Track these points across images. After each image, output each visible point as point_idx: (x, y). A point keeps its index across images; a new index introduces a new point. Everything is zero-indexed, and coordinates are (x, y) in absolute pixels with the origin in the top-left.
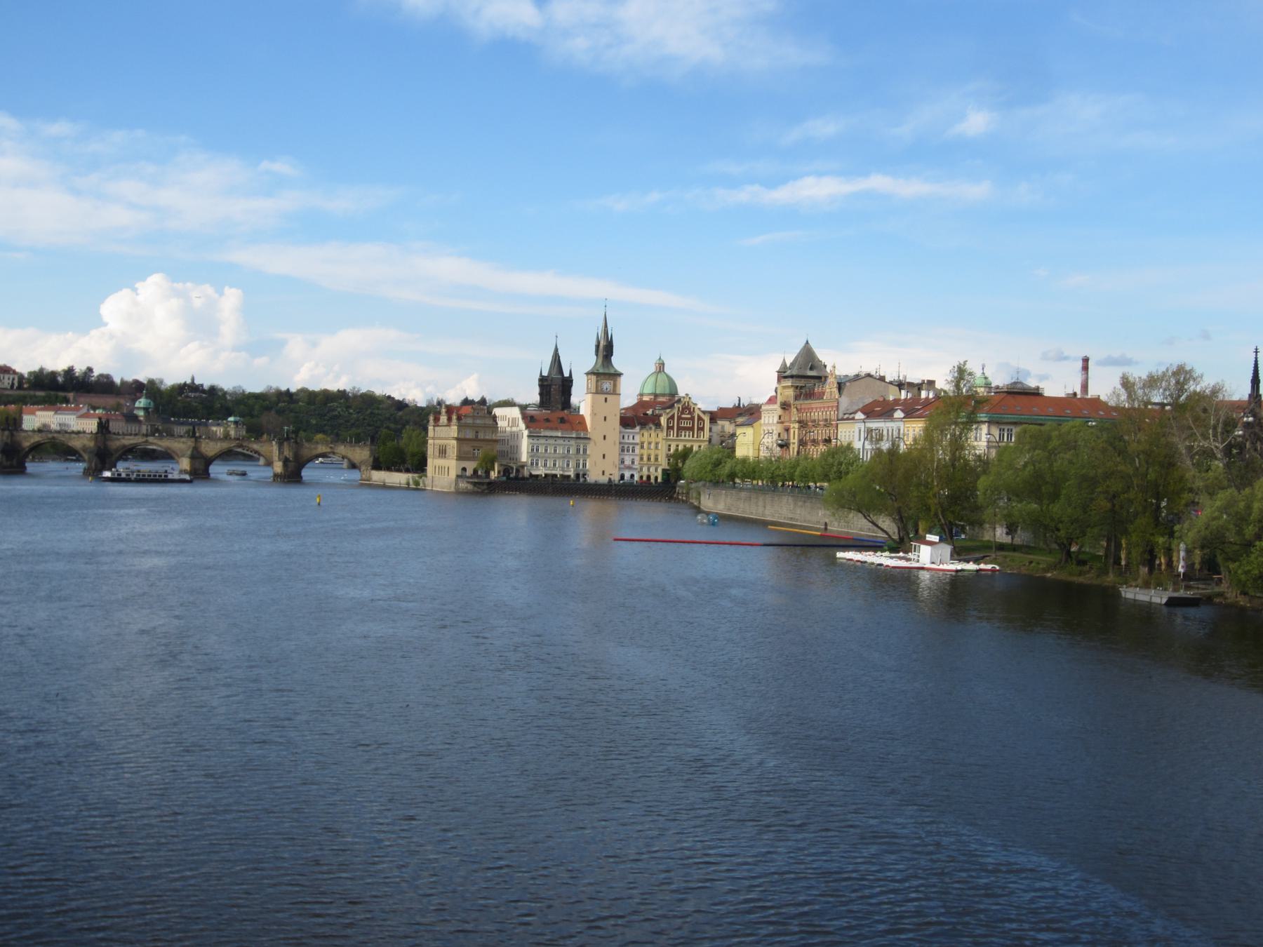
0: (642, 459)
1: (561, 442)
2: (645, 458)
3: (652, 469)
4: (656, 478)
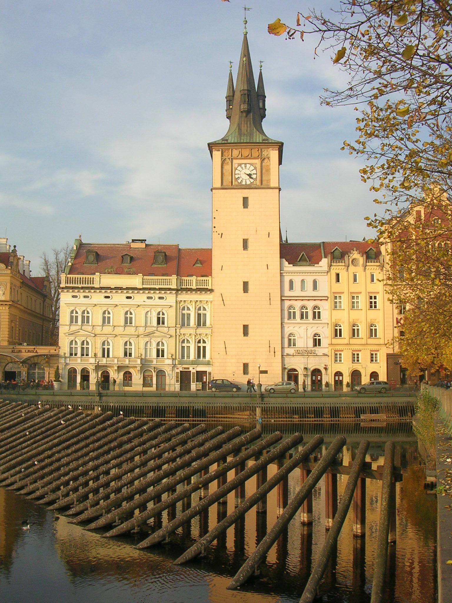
0: (338, 333)
1: (140, 298)
2: (346, 332)
3: (365, 356)
4: (374, 375)
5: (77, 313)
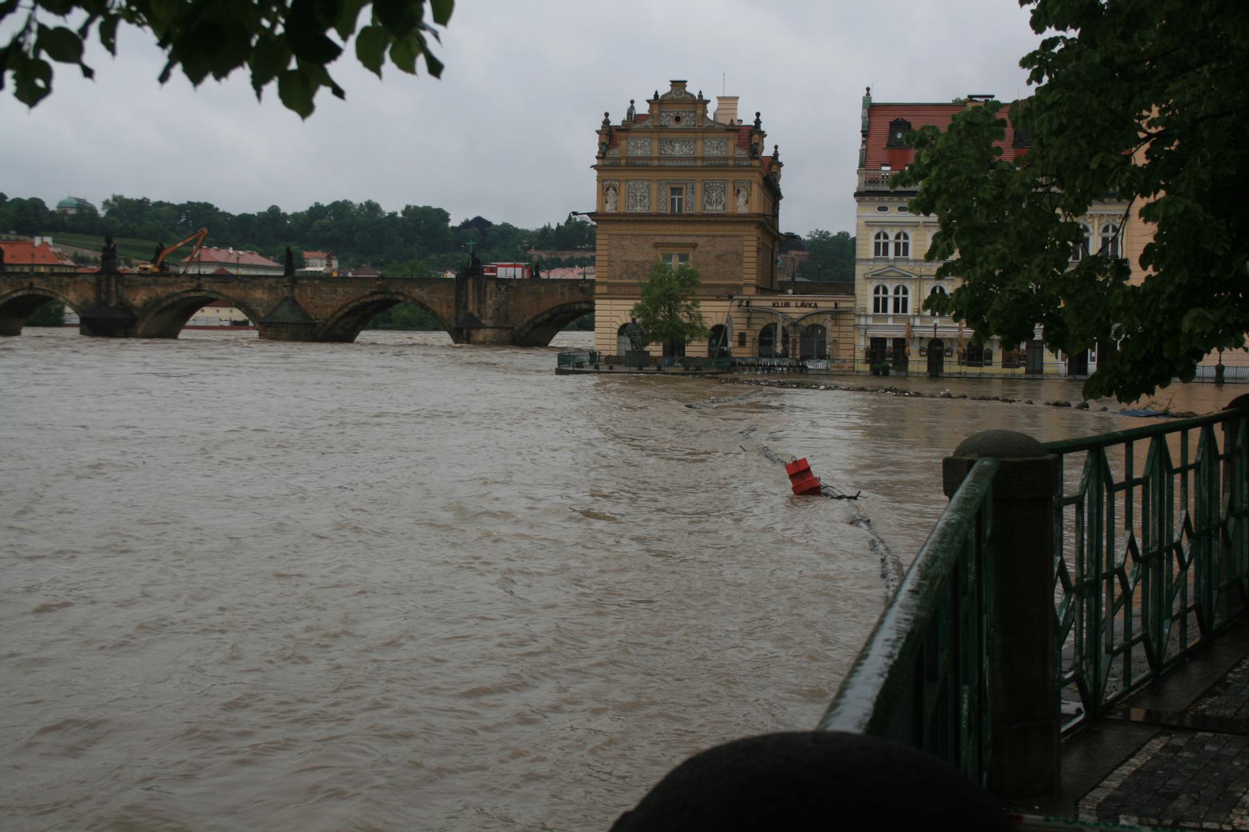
5: (886, 237)
